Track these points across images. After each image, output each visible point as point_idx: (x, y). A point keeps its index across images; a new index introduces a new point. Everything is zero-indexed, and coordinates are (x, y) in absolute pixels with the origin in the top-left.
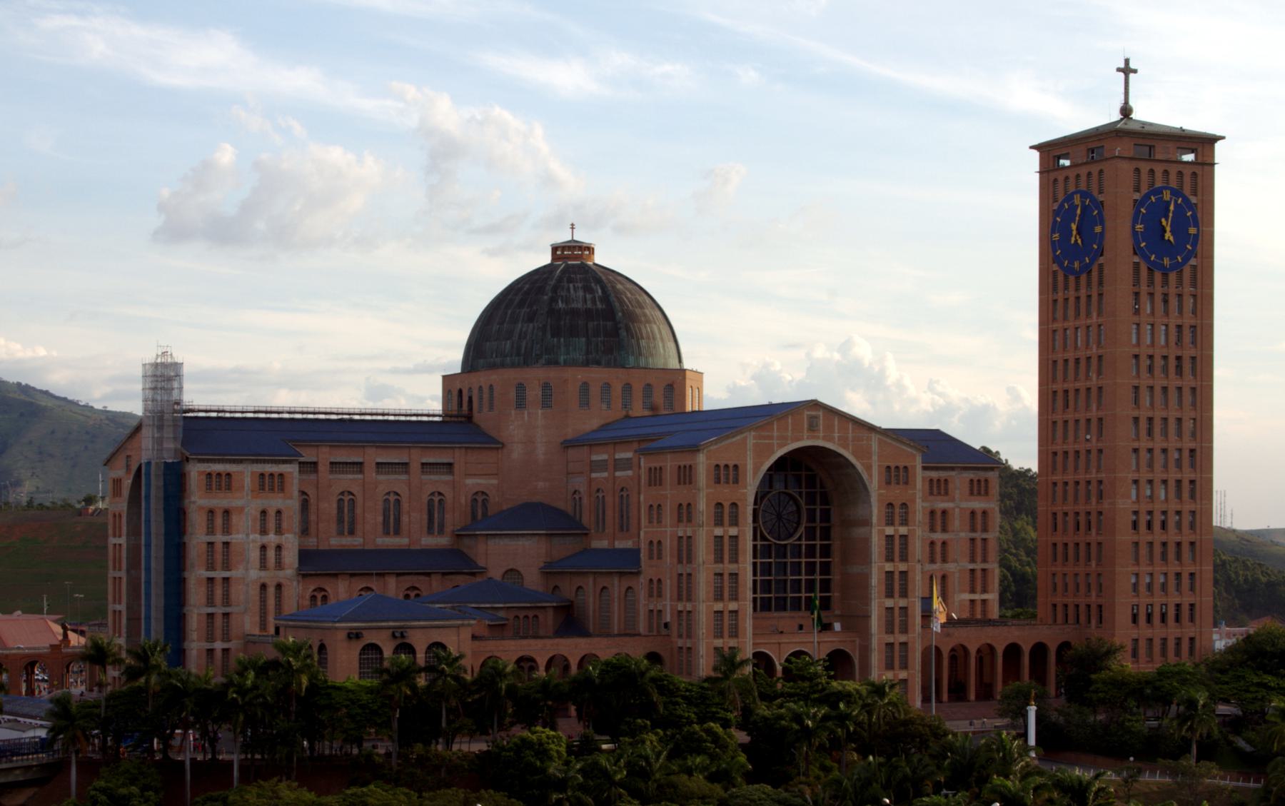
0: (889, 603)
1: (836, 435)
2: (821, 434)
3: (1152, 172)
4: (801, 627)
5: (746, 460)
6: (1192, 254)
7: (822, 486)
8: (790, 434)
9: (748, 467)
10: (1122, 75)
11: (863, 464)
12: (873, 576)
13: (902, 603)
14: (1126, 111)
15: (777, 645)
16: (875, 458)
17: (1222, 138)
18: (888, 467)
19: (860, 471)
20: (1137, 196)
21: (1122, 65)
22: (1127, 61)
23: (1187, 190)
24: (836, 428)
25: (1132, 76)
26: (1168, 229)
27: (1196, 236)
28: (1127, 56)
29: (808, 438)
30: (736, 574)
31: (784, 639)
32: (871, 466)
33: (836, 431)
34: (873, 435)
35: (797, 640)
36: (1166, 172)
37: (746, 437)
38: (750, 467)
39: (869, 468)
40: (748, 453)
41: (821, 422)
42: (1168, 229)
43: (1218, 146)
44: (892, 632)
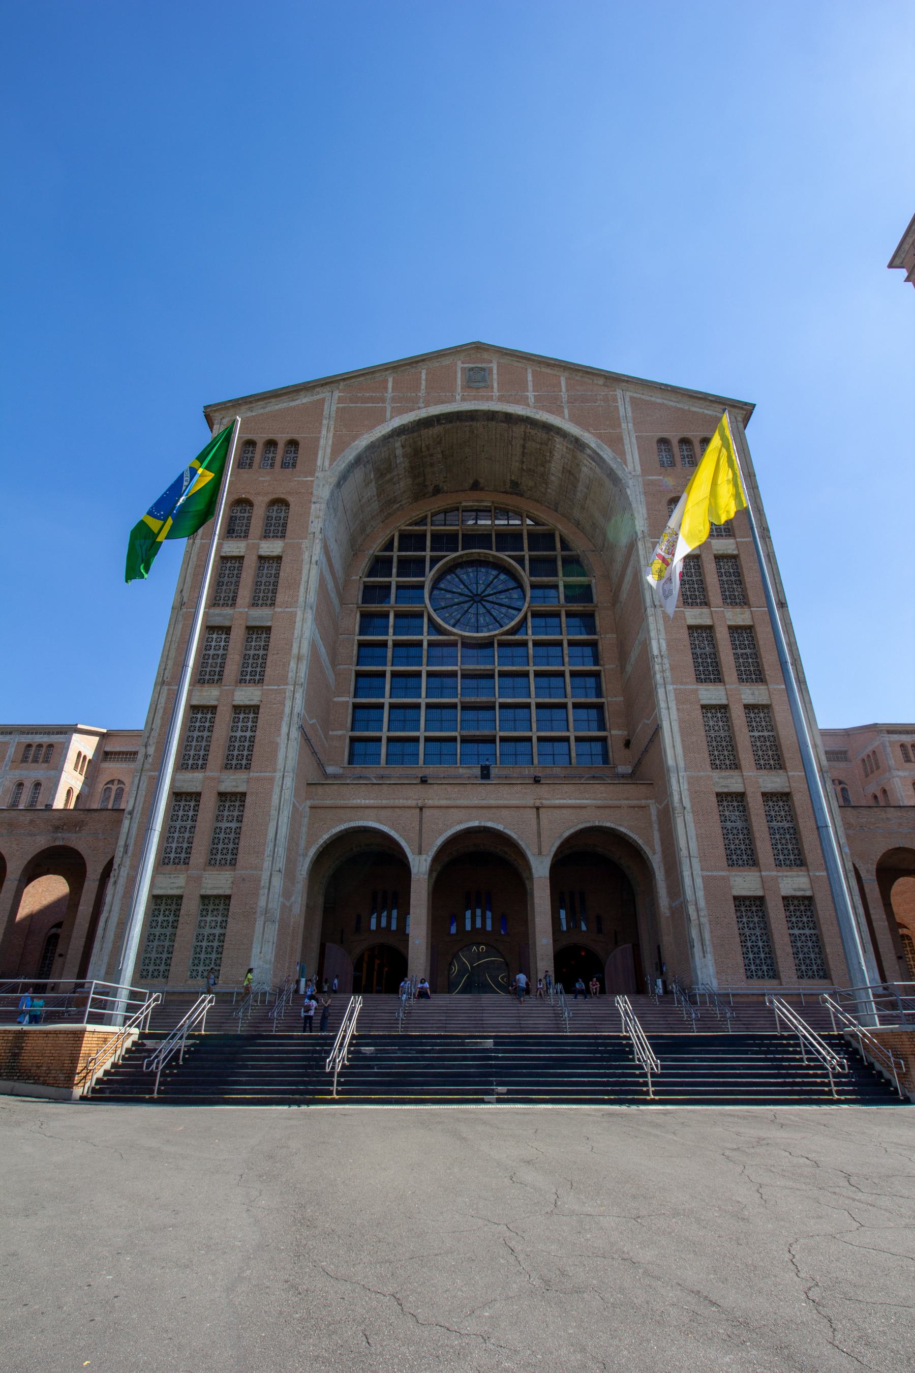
0: (712, 694)
1: (531, 395)
2: (496, 393)
4: (485, 773)
5: (320, 432)
7: (565, 546)
8: (422, 393)
9: (322, 442)
11: (599, 436)
12: (653, 634)
13: (752, 694)
15: (418, 810)
16: (627, 428)
18: (663, 442)
19: (593, 445)
24: (530, 384)
29: (463, 399)
30: (268, 629)
31: (435, 796)
32: (620, 439)
33: (530, 388)
34: (619, 393)
35: (476, 802)
37: (323, 400)
38: (326, 440)
39: (616, 442)
40: (325, 422)
41: (495, 376)
44: (736, 766)
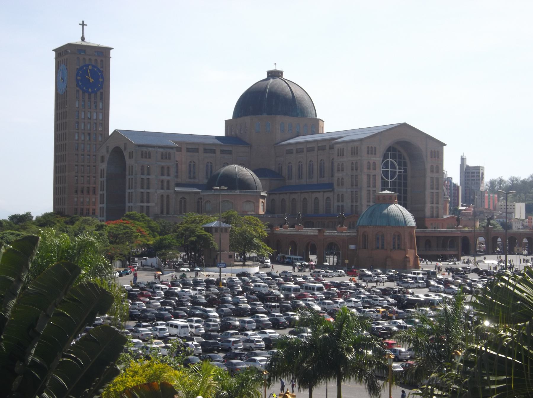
3: (84, 59)
6: (101, 88)
10: (81, 26)
14: (83, 39)
17: (112, 49)
20: (78, 67)
21: (81, 23)
22: (83, 22)
23: (99, 66)
25: (85, 26)
26: (90, 79)
27: (103, 82)
28: (83, 20)
36: (90, 59)
42: (90, 79)
43: (111, 51)
